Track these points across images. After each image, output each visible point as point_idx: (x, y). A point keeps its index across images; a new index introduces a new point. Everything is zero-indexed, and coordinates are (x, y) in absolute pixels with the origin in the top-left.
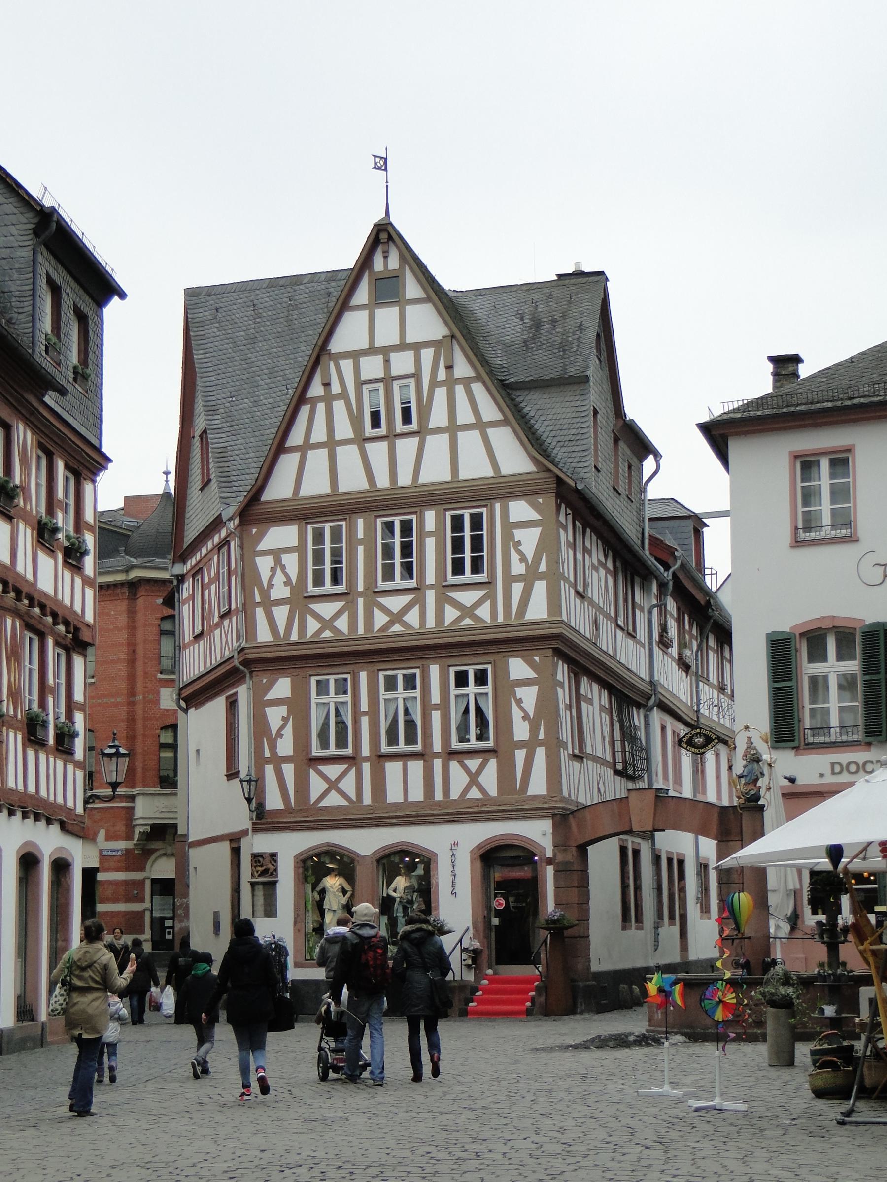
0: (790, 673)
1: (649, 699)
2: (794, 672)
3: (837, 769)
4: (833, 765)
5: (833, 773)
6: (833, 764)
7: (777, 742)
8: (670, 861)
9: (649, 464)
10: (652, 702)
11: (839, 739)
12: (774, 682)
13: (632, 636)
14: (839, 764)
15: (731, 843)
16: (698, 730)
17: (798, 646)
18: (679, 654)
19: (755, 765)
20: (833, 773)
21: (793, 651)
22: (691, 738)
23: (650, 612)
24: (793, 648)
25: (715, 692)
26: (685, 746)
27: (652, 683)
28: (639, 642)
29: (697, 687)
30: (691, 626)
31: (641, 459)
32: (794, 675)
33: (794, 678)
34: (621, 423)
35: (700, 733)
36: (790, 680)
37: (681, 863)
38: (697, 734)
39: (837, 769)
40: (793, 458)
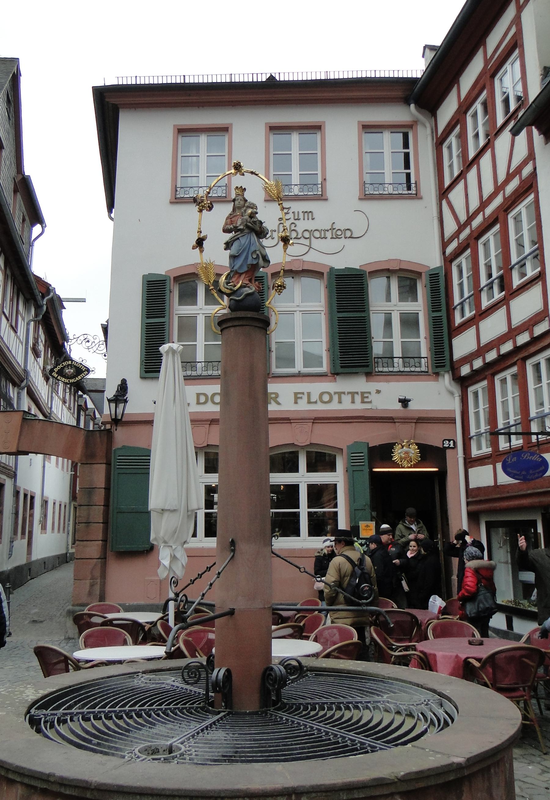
0: (163, 310)
1: (22, 381)
2: (167, 309)
3: (202, 399)
4: (198, 395)
5: (198, 403)
6: (198, 395)
7: (146, 372)
8: (25, 496)
9: (37, 229)
10: (23, 384)
11: (205, 373)
12: (148, 318)
13: (16, 332)
14: (205, 395)
15: (95, 466)
16: (70, 362)
17: (172, 288)
18: (44, 367)
19: (254, 237)
20: (198, 403)
21: (168, 292)
22: (62, 369)
23: (28, 324)
24: (168, 289)
25: (61, 403)
26: (56, 375)
27: (25, 371)
28: (18, 338)
29: (52, 393)
30: (51, 357)
31: (33, 225)
32: (167, 312)
33: (167, 314)
34: (20, 177)
35: (71, 365)
36: (164, 317)
37: (32, 498)
38: (69, 365)
39: (202, 399)
40: (176, 131)
